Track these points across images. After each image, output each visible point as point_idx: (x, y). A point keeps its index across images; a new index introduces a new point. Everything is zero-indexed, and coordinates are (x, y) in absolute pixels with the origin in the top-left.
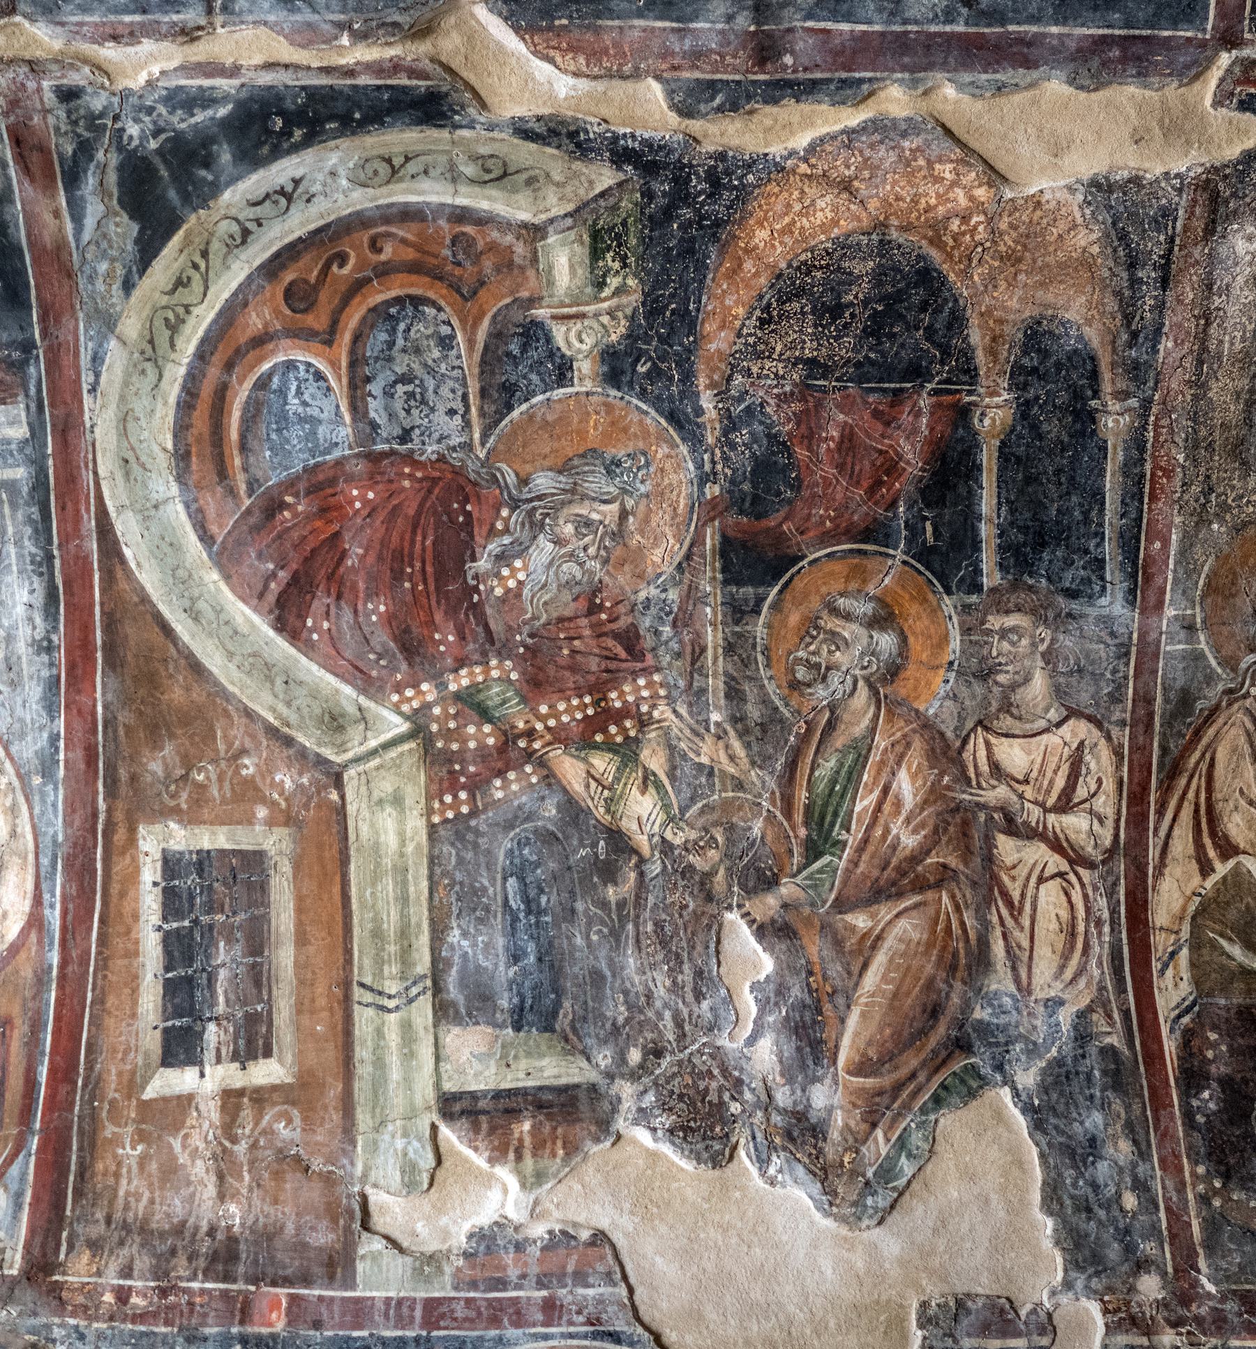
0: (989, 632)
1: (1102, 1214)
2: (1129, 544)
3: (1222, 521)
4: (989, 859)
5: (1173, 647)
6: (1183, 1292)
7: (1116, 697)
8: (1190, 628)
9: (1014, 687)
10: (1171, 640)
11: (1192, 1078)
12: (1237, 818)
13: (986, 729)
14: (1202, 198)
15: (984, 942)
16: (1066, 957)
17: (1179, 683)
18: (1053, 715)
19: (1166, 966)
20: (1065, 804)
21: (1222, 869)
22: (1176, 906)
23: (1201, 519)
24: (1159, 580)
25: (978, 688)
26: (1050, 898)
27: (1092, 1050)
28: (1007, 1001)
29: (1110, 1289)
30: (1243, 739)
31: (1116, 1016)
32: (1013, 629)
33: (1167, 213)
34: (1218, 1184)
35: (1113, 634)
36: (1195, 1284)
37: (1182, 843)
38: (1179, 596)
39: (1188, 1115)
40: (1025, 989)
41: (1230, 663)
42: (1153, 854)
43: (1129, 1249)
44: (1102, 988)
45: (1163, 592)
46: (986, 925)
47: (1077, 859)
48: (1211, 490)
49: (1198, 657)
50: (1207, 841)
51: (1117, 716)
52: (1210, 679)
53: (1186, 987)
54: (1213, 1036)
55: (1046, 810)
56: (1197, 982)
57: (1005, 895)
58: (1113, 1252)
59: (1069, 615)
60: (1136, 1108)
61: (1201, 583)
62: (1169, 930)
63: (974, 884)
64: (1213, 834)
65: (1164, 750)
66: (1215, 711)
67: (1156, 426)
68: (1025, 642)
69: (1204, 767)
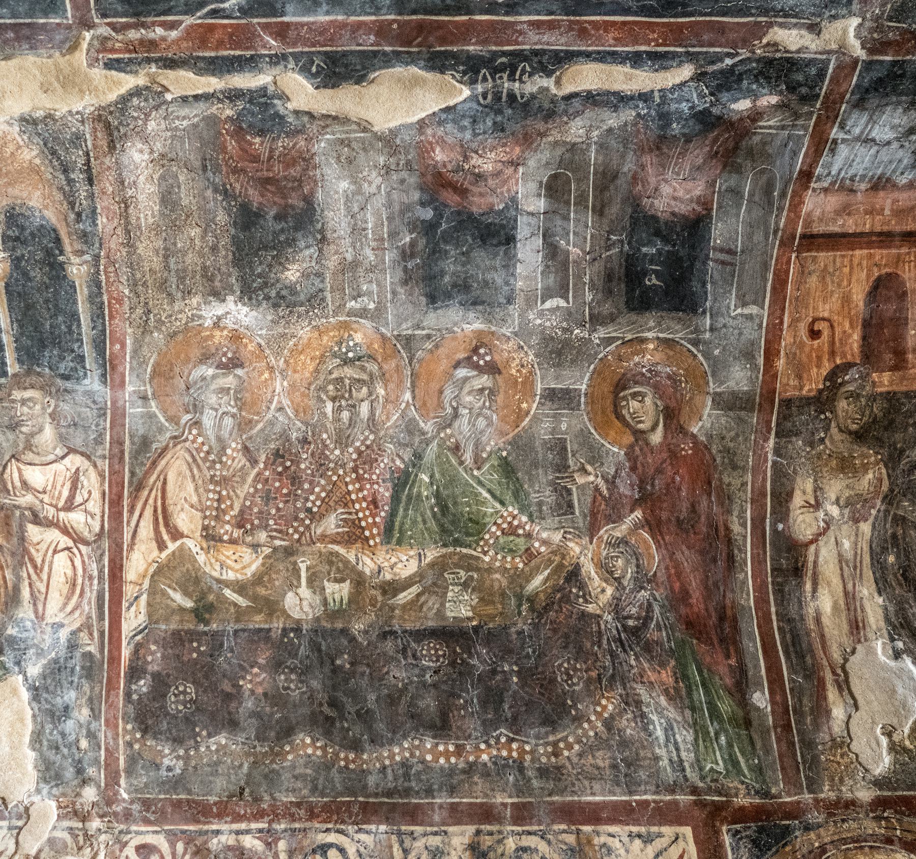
0: (14, 401)
1: (65, 751)
3: (160, 331)
4: (22, 539)
5: (134, 410)
6: (109, 798)
7: (99, 441)
8: (144, 398)
9: (33, 435)
10: (133, 405)
11: (135, 672)
12: (183, 515)
13: (18, 460)
15: (17, 589)
16: (68, 599)
17: (141, 432)
18: (59, 452)
19: (131, 605)
20: (69, 506)
21: (172, 546)
22: (142, 568)
23: (145, 329)
24: (120, 369)
25: (11, 436)
26: (61, 563)
27: (78, 654)
28: (28, 624)
29: (64, 795)
30: (185, 467)
31: (96, 634)
32: (29, 399)
34: (138, 736)
35: (94, 402)
36: (116, 793)
37: (146, 530)
38: (134, 378)
39: (128, 695)
40: (40, 617)
41: (174, 420)
42: (127, 537)
43: (80, 771)
44: (89, 617)
45: (123, 375)
46: (19, 578)
47: (78, 539)
49: (151, 416)
50: (162, 529)
51: (99, 452)
52: (161, 430)
53: (142, 619)
54: (153, 648)
55: (58, 510)
56: (150, 615)
57: (32, 560)
58: (69, 773)
59: (65, 390)
60: (97, 689)
61: (149, 370)
62: (136, 583)
63: (13, 554)
64: (167, 525)
65: (133, 474)
66: (165, 449)
68: (38, 407)
69: (159, 484)
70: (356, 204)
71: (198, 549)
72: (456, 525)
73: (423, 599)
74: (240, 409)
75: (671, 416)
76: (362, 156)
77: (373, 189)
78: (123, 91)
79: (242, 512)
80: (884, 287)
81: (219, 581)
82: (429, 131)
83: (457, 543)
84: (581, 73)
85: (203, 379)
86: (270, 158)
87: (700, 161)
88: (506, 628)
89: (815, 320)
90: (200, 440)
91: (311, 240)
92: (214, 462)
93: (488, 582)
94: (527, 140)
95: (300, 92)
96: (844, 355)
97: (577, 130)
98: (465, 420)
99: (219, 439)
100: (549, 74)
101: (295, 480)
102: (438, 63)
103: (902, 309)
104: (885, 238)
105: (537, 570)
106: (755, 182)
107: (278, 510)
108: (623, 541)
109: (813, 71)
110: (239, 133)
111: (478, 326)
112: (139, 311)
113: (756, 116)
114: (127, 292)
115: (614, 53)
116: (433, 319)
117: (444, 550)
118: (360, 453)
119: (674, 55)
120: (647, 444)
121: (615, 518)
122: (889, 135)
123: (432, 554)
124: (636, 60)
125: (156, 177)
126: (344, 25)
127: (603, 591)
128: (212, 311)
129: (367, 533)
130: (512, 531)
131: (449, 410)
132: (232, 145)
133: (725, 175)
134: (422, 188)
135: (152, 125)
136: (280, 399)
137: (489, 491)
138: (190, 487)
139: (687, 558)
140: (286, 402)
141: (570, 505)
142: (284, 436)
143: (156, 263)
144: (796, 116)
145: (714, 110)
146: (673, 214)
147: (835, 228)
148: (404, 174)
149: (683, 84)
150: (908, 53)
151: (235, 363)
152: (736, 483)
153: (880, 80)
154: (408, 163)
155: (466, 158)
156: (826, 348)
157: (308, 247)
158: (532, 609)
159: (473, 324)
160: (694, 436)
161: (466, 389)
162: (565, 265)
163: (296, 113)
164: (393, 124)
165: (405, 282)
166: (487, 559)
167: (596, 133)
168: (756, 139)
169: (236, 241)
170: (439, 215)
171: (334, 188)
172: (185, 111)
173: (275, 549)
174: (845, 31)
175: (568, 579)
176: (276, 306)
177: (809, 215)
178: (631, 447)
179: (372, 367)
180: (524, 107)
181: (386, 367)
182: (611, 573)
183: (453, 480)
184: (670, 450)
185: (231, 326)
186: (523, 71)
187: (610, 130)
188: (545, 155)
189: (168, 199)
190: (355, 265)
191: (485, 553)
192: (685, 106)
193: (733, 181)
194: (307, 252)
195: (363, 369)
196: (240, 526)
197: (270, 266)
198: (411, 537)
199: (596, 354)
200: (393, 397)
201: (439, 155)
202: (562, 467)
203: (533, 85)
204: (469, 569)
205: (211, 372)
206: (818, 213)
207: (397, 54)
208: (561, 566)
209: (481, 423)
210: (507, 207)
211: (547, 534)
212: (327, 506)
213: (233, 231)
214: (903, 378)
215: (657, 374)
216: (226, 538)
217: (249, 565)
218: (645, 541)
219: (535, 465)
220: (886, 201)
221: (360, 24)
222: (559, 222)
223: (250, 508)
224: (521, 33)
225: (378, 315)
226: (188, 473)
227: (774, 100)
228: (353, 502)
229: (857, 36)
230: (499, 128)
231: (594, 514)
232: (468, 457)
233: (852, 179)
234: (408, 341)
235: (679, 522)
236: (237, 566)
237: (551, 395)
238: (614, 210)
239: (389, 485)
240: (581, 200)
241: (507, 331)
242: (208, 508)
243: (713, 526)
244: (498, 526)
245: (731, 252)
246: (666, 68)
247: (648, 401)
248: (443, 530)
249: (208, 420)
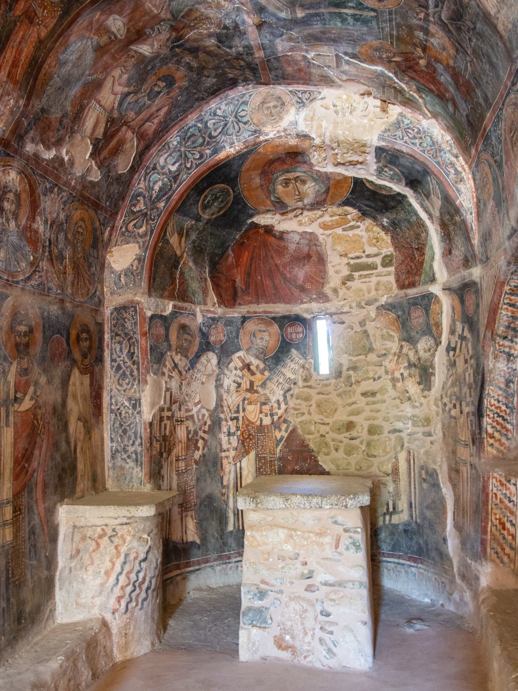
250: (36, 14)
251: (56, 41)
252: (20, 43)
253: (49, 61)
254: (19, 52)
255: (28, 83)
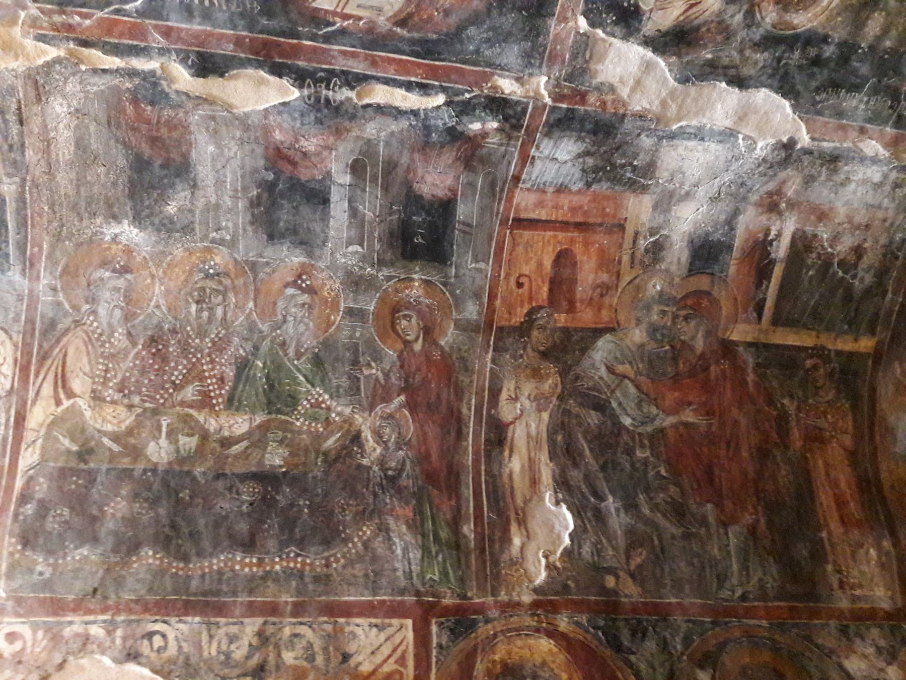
2: (22, 248)
3: (70, 240)
8: (54, 289)
10: (45, 295)
12: (77, 381)
14: (29, 82)
21: (66, 403)
30: (81, 344)
33: (12, 90)
37: (47, 389)
38: (48, 274)
42: (31, 394)
48: (63, 225)
49: (59, 304)
50: (61, 391)
51: (16, 328)
52: (66, 314)
61: (59, 269)
64: (64, 387)
65: (40, 346)
66: (67, 330)
67: (31, 193)
69: (61, 356)
70: (220, 168)
71: (86, 407)
72: (278, 398)
73: (249, 451)
74: (127, 304)
75: (428, 331)
76: (223, 130)
77: (232, 154)
78: (48, 58)
79: (123, 380)
80: (563, 258)
81: (99, 431)
82: (272, 118)
83: (279, 411)
84: (373, 90)
85: (102, 279)
86: (158, 122)
87: (450, 161)
88: (305, 474)
89: (520, 276)
90: (95, 324)
91: (186, 186)
92: (105, 342)
93: (297, 441)
94: (339, 133)
95: (182, 77)
96: (537, 301)
97: (371, 129)
98: (291, 325)
99: (110, 325)
100: (352, 88)
101: (165, 360)
102: (278, 71)
103: (574, 274)
104: (564, 225)
105: (332, 433)
106: (484, 181)
107: (150, 380)
108: (391, 416)
109: (519, 109)
110: (135, 101)
111: (302, 259)
112: (55, 224)
113: (484, 135)
114: (46, 208)
115: (395, 80)
116: (270, 252)
117: (269, 417)
118: (214, 343)
119: (433, 87)
120: (412, 350)
121: (387, 400)
122: (567, 157)
123: (259, 419)
124: (409, 86)
125: (72, 126)
126: (211, 34)
127: (375, 450)
128: (111, 230)
129: (214, 401)
130: (318, 405)
131: (280, 317)
132: (130, 109)
133: (465, 173)
134: (267, 159)
135: (69, 88)
136: (157, 297)
137: (305, 376)
138: (85, 359)
139: (432, 431)
140: (162, 302)
141: (358, 389)
142: (159, 327)
143: (71, 192)
144: (510, 138)
145: (458, 128)
146: (433, 196)
147: (532, 216)
148: (255, 146)
149: (438, 107)
150: (576, 104)
151: (125, 270)
152: (467, 380)
153: (559, 120)
154: (256, 138)
155: (297, 141)
156: (526, 293)
157: (183, 190)
158: (325, 461)
159: (297, 259)
160: (442, 348)
161: (293, 303)
162: (363, 222)
163: (177, 92)
164: (246, 109)
165: (252, 223)
166: (298, 424)
167: (383, 134)
168: (484, 151)
169: (131, 182)
170: (277, 178)
171: (204, 151)
172: (95, 79)
173: (145, 410)
174: (538, 85)
175: (352, 441)
176: (159, 231)
177: (518, 205)
178: (402, 352)
179: (227, 282)
180: (336, 109)
181: (236, 282)
182: (381, 437)
183: (279, 367)
184: (427, 356)
185: (124, 242)
186: (335, 84)
187: (392, 133)
188: (350, 145)
189: (80, 144)
190: (217, 206)
191: (298, 420)
192: (440, 123)
193: (471, 177)
194: (182, 194)
195: (220, 282)
196: (121, 391)
197: (156, 201)
198: (246, 406)
199: (381, 286)
200: (240, 304)
201: (278, 136)
202: (355, 363)
203: (344, 94)
204: (285, 430)
205: (107, 274)
206: (523, 204)
207: (249, 59)
208: (348, 431)
209: (302, 328)
210: (324, 178)
211: (341, 409)
212: (187, 380)
213: (129, 172)
214: (574, 319)
215: (420, 303)
216: (108, 399)
217: (124, 421)
218: (405, 416)
219: (337, 359)
220: (565, 201)
221: (223, 35)
222: (359, 193)
223: (129, 378)
224: (333, 57)
225: (232, 244)
226: (83, 348)
227: (495, 125)
228: (207, 378)
229: (545, 89)
230: (319, 121)
231: (374, 396)
232: (291, 352)
233: (544, 184)
234: (253, 266)
235: (429, 406)
236: (115, 421)
237: (350, 312)
238: (395, 189)
239: (234, 367)
240: (374, 179)
241: (321, 264)
242: (98, 376)
243: (451, 409)
244: (309, 401)
245: (469, 225)
246: (428, 95)
247: (414, 320)
248: (270, 403)
249: (102, 311)
250: (821, 429)
251: (872, 438)
252: (828, 474)
253: (883, 467)
254: (835, 484)
255: (877, 513)
